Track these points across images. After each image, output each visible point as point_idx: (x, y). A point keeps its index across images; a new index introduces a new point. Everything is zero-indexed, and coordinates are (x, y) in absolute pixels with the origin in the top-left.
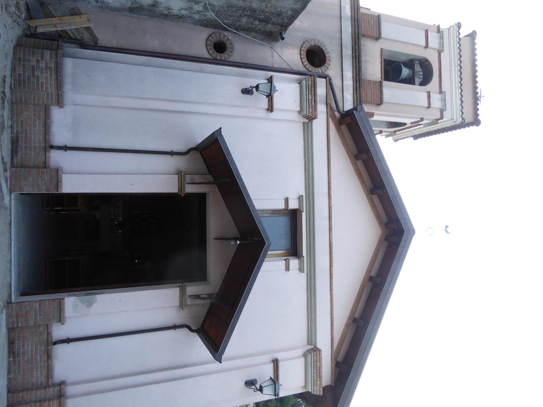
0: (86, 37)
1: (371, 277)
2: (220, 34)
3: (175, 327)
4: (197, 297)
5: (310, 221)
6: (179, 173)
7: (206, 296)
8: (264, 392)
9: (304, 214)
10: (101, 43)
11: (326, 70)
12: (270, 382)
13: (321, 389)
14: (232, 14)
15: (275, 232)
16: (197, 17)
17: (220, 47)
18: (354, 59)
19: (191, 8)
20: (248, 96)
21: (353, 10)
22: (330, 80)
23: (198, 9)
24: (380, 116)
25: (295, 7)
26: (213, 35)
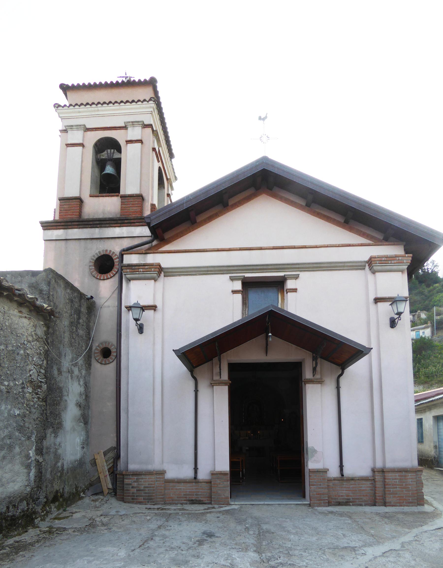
0: (111, 455)
1: (306, 205)
2: (95, 353)
3: (338, 388)
4: (314, 369)
5: (253, 269)
6: (212, 385)
7: (314, 362)
8: (402, 311)
9: (247, 275)
10: (114, 444)
11: (116, 255)
12: (394, 306)
13: (407, 255)
14: (77, 343)
15: (262, 302)
16: (84, 372)
17: (106, 353)
18: (103, 226)
19: (78, 377)
20: (145, 328)
21: (58, 227)
22: (124, 250)
23: (77, 371)
24: (153, 197)
25: (62, 286)
26: (97, 359)
